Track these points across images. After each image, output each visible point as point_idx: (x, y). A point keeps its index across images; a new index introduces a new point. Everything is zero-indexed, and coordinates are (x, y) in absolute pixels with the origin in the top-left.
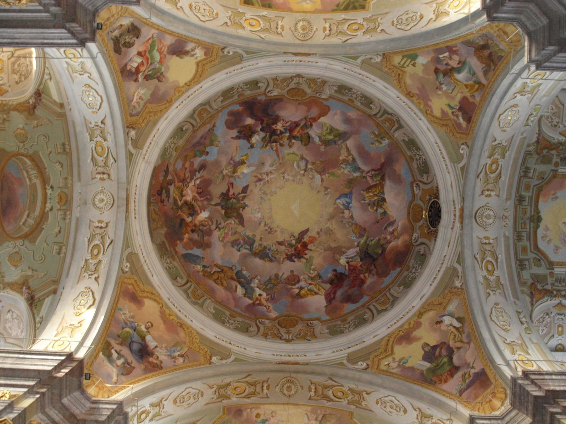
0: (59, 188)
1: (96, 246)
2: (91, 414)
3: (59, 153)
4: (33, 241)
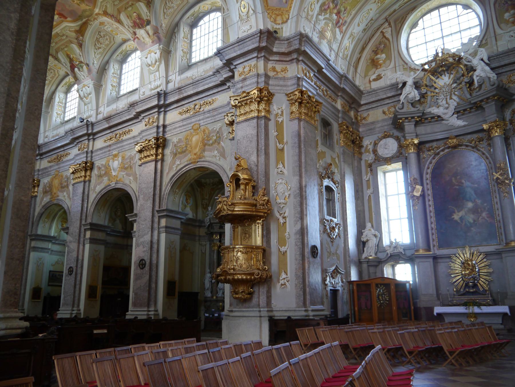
2: (291, 46)
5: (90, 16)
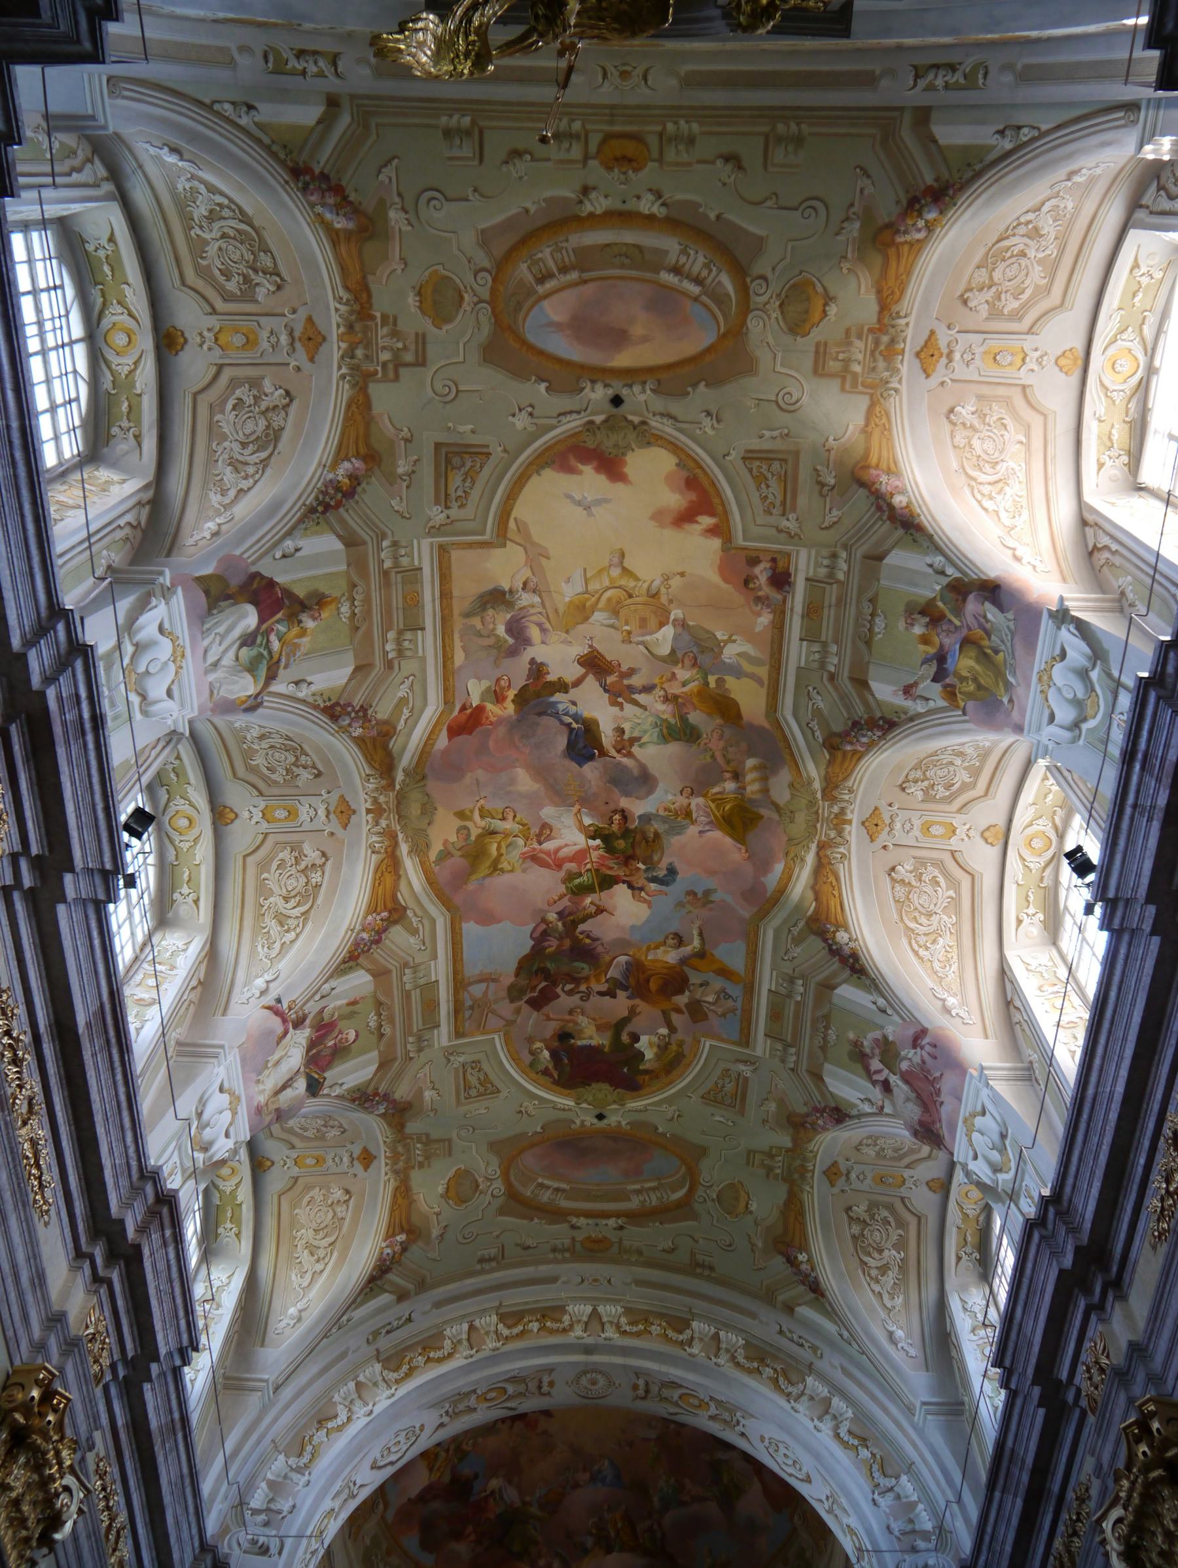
0: (621, 1239)
1: (504, 1390)
3: (693, 1254)
4: (502, 1211)
5: (399, 803)
